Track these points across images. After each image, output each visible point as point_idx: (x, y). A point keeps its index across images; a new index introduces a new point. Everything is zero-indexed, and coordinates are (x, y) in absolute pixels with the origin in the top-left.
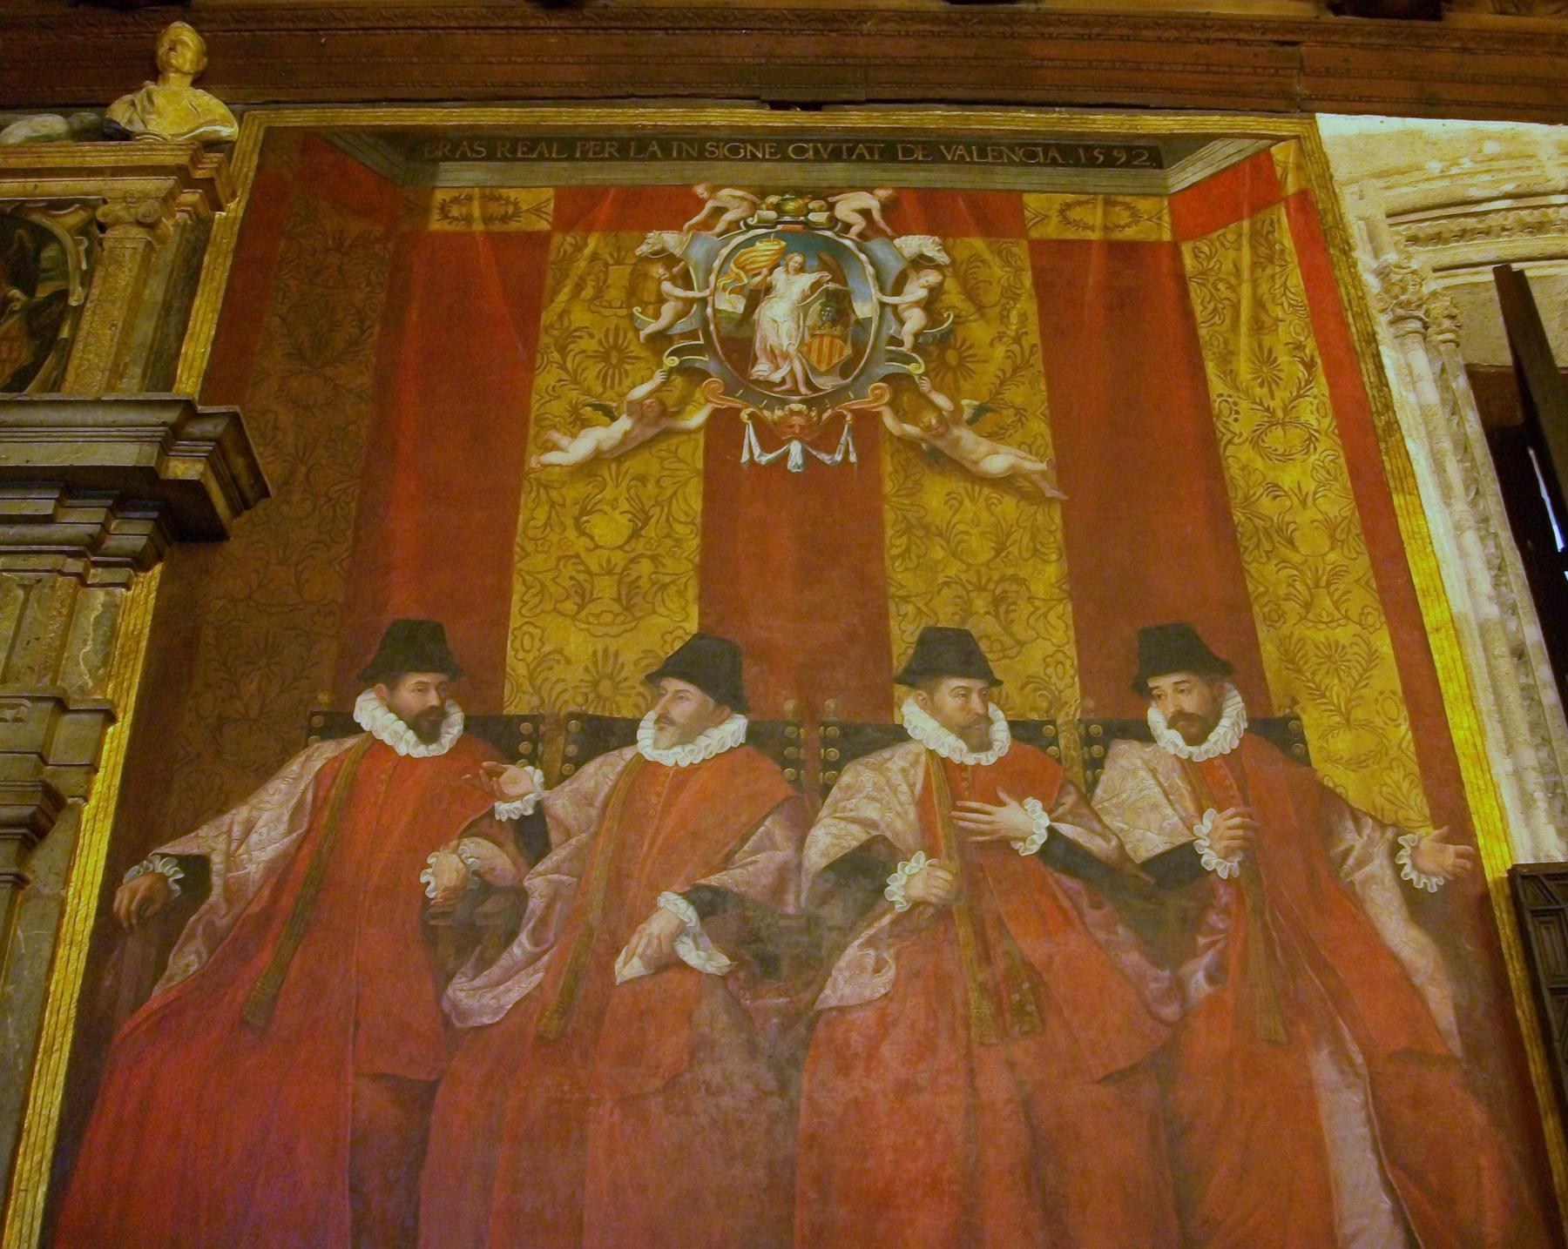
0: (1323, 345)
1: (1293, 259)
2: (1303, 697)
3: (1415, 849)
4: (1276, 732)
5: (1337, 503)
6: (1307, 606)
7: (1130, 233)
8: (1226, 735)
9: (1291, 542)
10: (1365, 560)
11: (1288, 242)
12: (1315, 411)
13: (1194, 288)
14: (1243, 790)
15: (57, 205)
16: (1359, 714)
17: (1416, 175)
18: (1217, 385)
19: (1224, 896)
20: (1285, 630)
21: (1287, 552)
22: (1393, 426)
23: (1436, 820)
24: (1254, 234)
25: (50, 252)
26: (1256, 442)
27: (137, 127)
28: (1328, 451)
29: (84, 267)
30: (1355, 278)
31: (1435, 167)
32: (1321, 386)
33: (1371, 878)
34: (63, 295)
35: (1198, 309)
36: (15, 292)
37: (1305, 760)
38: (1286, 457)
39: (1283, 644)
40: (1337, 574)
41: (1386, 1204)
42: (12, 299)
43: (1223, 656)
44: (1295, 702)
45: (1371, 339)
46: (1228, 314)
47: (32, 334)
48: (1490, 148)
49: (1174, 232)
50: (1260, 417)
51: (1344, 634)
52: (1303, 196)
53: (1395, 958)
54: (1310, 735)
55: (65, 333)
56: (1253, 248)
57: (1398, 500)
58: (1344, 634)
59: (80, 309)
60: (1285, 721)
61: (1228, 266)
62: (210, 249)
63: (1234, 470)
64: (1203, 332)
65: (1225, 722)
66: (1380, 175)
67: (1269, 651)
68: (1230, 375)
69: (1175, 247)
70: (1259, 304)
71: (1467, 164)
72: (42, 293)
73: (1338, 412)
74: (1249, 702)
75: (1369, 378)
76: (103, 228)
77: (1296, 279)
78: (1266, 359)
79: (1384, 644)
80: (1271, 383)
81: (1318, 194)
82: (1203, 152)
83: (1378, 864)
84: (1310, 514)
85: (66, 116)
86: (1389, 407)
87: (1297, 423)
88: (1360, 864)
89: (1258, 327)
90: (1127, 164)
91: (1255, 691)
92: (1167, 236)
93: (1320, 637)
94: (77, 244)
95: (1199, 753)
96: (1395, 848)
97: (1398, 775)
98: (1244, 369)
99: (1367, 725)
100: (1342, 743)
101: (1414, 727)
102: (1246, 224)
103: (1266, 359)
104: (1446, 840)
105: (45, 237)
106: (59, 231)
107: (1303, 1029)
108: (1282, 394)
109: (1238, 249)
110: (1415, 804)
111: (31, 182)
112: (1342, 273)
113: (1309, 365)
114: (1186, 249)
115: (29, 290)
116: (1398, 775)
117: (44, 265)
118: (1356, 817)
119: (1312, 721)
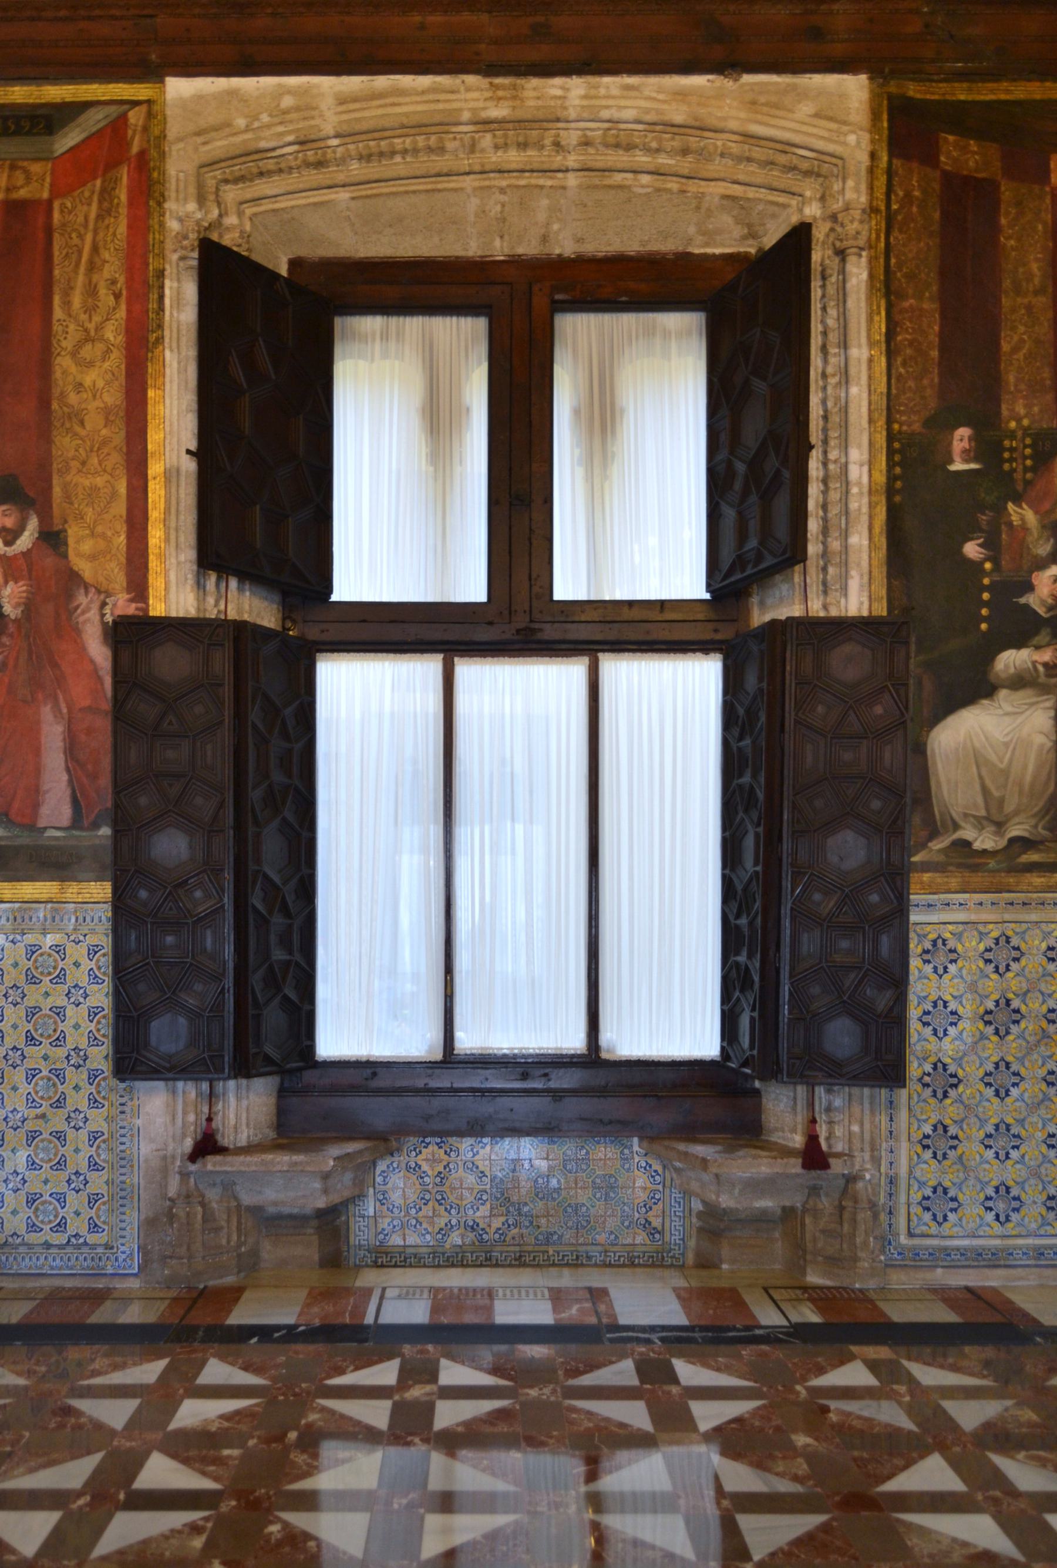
0: (130, 280)
1: (123, 211)
2: (70, 519)
3: (115, 605)
4: (52, 538)
5: (113, 397)
6: (84, 463)
7: (23, 193)
8: (25, 541)
9: (82, 423)
10: (123, 434)
11: (124, 197)
12: (113, 333)
13: (56, 236)
14: (30, 571)
16: (99, 529)
17: (227, 130)
18: (58, 313)
19: (12, 628)
20: (68, 478)
21: (78, 429)
22: (160, 340)
23: (129, 590)
24: (103, 190)
26: (74, 354)
28: (116, 360)
30: (162, 224)
31: (241, 122)
32: (122, 313)
33: (88, 620)
35: (56, 253)
37: (65, 556)
38: (90, 364)
39: (65, 487)
40: (105, 442)
41: (65, 777)
43: (32, 494)
44: (66, 522)
45: (161, 274)
46: (74, 257)
48: (287, 102)
49: (51, 191)
50: (80, 336)
51: (99, 481)
52: (142, 154)
53: (92, 661)
54: (71, 541)
56: (100, 202)
57: (151, 393)
58: (99, 481)
60: (58, 534)
61: (81, 219)
63: (58, 374)
64: (57, 272)
65: (26, 533)
66: (198, 134)
67: (57, 491)
68: (67, 304)
69: (49, 203)
70: (95, 249)
71: (265, 118)
73: (129, 331)
74: (41, 522)
75: (153, 305)
77: (122, 229)
78: (91, 291)
79: (122, 489)
80: (90, 310)
81: (153, 153)
82: (82, 119)
83: (93, 614)
84: (98, 403)
86: (160, 326)
87: (102, 339)
88: (83, 613)
89: (92, 267)
90: (29, 133)
91: (45, 517)
92: (46, 195)
93: (87, 483)
95: (10, 551)
96: (104, 604)
97: (113, 564)
98: (77, 301)
99: (103, 536)
100: (87, 547)
101: (128, 538)
102: (98, 182)
103: (91, 291)
104: (132, 600)
107: (40, 696)
108: (97, 319)
109: (89, 205)
110: (119, 579)
112: (154, 222)
113: (117, 296)
114: (56, 205)
116: (113, 564)
118: (87, 587)
119: (73, 532)
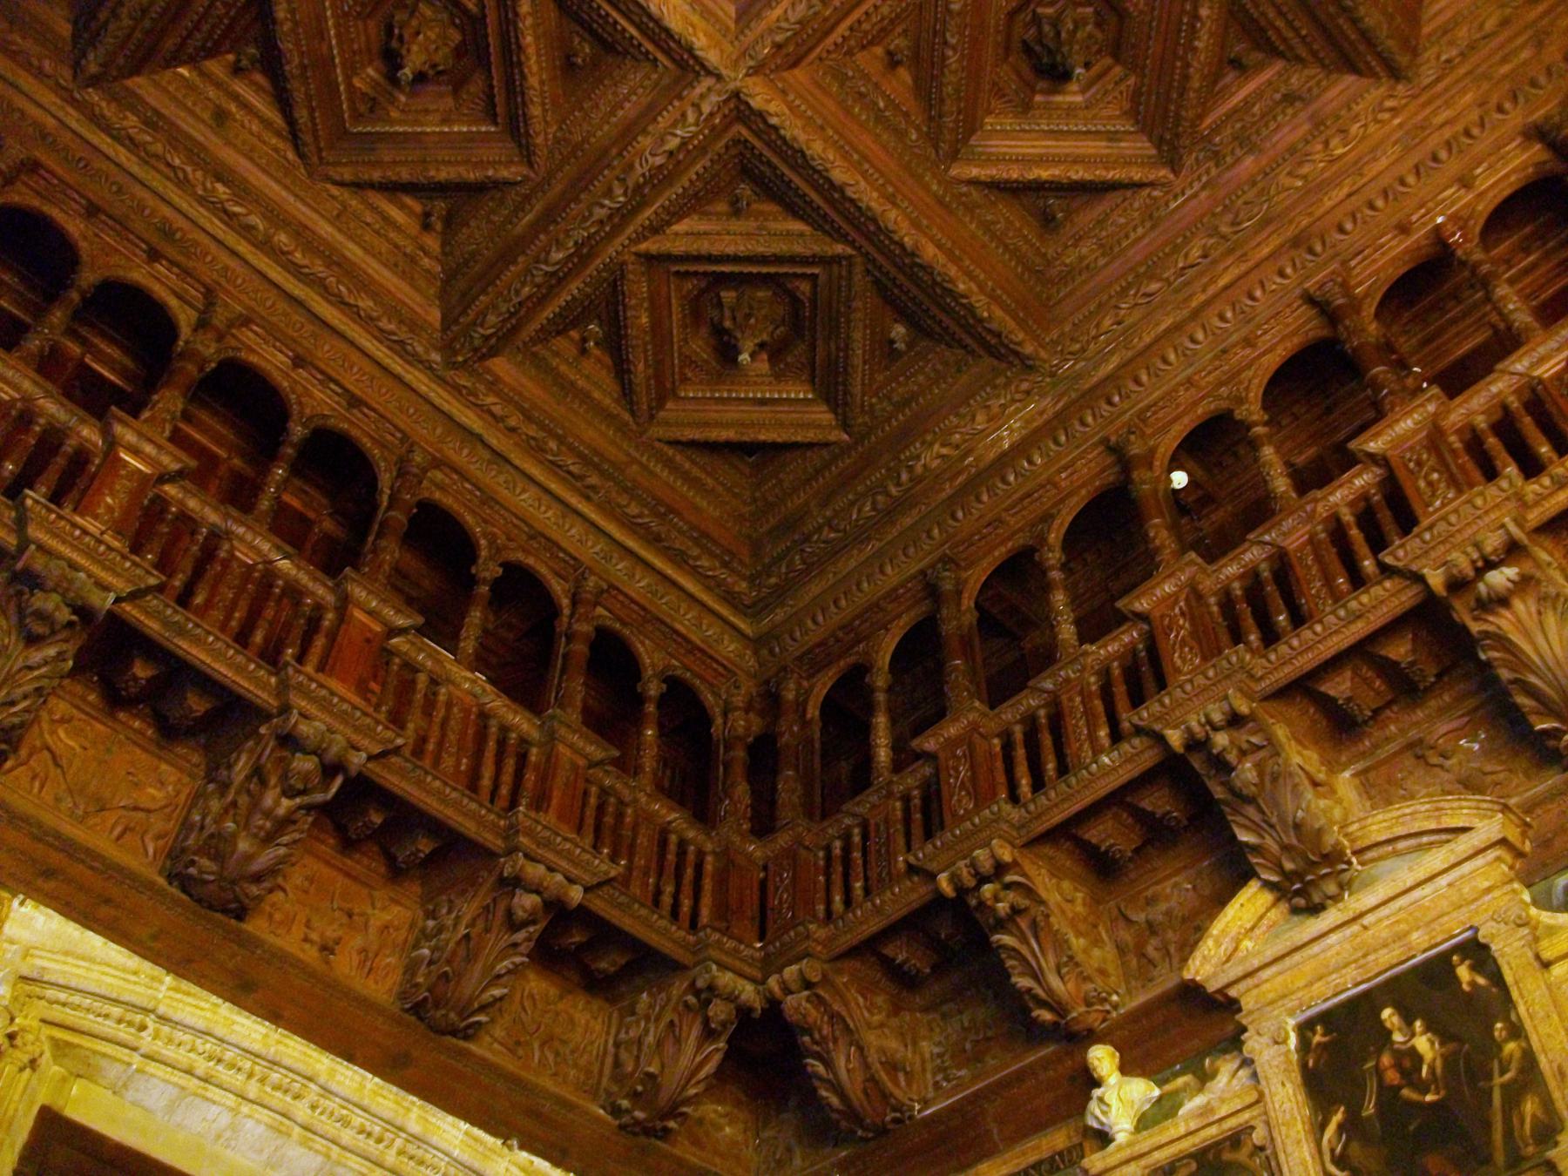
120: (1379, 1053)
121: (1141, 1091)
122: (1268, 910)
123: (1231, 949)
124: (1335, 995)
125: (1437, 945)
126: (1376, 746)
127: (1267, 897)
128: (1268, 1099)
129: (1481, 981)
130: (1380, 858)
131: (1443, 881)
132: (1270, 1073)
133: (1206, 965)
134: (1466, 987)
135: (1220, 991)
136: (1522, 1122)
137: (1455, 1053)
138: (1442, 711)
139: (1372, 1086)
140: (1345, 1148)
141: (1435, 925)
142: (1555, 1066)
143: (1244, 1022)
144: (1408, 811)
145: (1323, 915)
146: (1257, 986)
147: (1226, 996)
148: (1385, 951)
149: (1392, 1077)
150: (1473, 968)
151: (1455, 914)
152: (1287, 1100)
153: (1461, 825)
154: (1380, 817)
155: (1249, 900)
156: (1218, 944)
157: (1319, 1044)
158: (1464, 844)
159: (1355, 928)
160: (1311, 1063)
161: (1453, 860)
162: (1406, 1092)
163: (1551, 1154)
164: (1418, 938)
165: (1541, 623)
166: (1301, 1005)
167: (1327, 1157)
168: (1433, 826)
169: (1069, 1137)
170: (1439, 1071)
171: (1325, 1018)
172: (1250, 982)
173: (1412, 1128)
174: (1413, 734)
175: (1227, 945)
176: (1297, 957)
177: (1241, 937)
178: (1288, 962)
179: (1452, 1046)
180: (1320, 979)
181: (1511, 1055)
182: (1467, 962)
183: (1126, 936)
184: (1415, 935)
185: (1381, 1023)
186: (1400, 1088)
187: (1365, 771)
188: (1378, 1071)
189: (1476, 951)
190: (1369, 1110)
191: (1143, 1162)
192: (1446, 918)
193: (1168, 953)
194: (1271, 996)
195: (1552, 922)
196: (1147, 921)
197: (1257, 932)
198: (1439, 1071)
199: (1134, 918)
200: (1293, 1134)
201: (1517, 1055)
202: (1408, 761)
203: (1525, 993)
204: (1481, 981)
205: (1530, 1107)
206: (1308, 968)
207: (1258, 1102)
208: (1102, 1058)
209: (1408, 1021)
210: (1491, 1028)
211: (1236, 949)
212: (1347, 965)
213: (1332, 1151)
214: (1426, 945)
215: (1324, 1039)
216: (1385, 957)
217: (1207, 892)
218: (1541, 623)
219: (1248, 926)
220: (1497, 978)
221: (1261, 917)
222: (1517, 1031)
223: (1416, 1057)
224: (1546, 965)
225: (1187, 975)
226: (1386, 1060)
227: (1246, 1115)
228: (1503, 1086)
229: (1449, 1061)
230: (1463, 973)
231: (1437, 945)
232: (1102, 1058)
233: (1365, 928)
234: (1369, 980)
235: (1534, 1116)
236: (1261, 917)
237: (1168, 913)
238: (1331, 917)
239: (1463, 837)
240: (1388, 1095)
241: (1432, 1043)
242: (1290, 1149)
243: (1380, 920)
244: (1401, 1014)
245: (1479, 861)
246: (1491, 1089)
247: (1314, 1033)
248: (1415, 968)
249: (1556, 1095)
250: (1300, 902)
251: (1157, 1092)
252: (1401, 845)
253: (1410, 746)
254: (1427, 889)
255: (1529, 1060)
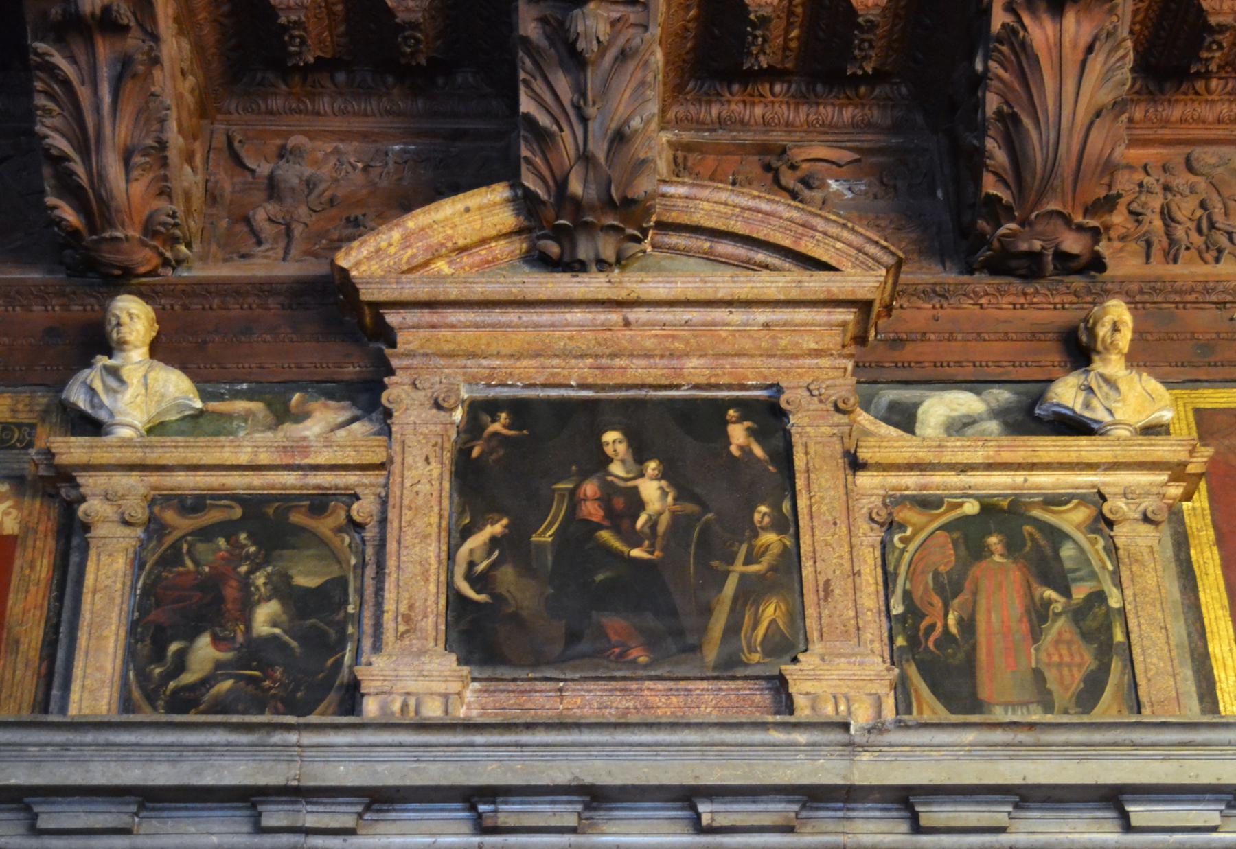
15: (1053, 501)
25: (1067, 551)
27: (1100, 414)
29: (1110, 567)
34: (1099, 597)
36: (1050, 593)
42: (1050, 602)
47: (1087, 636)
55: (1119, 637)
59: (1122, 611)
62: (1192, 542)
72: (1080, 593)
76: (1110, 524)
85: (978, 393)
94: (1093, 543)
105: (1057, 536)
106: (1068, 528)
111: (1019, 478)
115: (1066, 592)
117: (1068, 565)
120: (584, 476)
121: (175, 386)
122: (498, 237)
123: (420, 259)
124: (545, 386)
125: (717, 387)
126: (721, 123)
127: (507, 219)
128: (396, 468)
129: (758, 451)
130: (686, 252)
131: (762, 316)
132: (411, 440)
133: (375, 260)
134: (734, 449)
135: (376, 306)
136: (756, 624)
137: (691, 519)
138: (828, 130)
139: (558, 513)
140: (494, 566)
141: (727, 363)
142: (822, 579)
143: (395, 363)
144: (764, 206)
145: (583, 277)
146: (433, 326)
147: (381, 318)
148: (643, 362)
149: (592, 510)
150: (751, 432)
151: (758, 361)
152: (424, 480)
153: (825, 258)
154: (724, 196)
155: (480, 208)
156: (406, 242)
157: (496, 434)
158: (817, 284)
159: (615, 317)
160: (476, 452)
161: (794, 294)
162: (605, 535)
163: (788, 669)
164: (695, 368)
165: (1084, 63)
166: (491, 377)
167: (460, 570)
168: (787, 242)
169: (14, 411)
170: (661, 528)
171: (519, 409)
172: (426, 316)
173: (600, 577)
174: (778, 137)
175: (417, 251)
176: (512, 316)
177: (442, 247)
178: (496, 316)
179: (691, 508)
180: (537, 355)
181: (767, 547)
182: (747, 424)
183: (227, 184)
184: (694, 362)
185: (600, 445)
186: (600, 527)
187: (688, 148)
188: (574, 499)
189: (769, 415)
190: (545, 536)
191: (153, 479)
192: (744, 361)
193: (289, 233)
194: (447, 347)
195: (872, 428)
196: (271, 178)
197: (466, 259)
198: (661, 528)
199: (250, 163)
200: (420, 524)
201: (776, 549)
202: (753, 165)
203: (814, 487)
204: (758, 451)
205: (771, 611)
206: (519, 339)
207: (381, 466)
208: (134, 318)
209: (640, 455)
210: (753, 509)
211: (426, 264)
212: (582, 356)
213: (471, 564)
214: (703, 380)
215: (505, 431)
216: (638, 370)
217: (384, 183)
218: (1084, 63)
219: (461, 242)
220: (784, 457)
221: (483, 241)
222: (788, 524)
223: (636, 503)
224: (855, 464)
225: (343, 261)
226: (590, 488)
227: (351, 478)
228: (743, 577)
229: (680, 524)
230: (738, 434)
231: (717, 387)
232: (134, 318)
233: (627, 324)
234: (603, 387)
235: (773, 622)
236: (483, 241)
237: (310, 184)
238: (593, 284)
239: (824, 275)
240: (577, 534)
241: (665, 495)
242: (408, 539)
243: (653, 324)
244: (630, 445)
245: (821, 315)
246: (727, 573)
247: (494, 421)
248: (672, 400)
249: (811, 611)
250: (553, 249)
251: (198, 404)
252: (725, 248)
253: (764, 149)
254: (738, 316)
255: (791, 561)
